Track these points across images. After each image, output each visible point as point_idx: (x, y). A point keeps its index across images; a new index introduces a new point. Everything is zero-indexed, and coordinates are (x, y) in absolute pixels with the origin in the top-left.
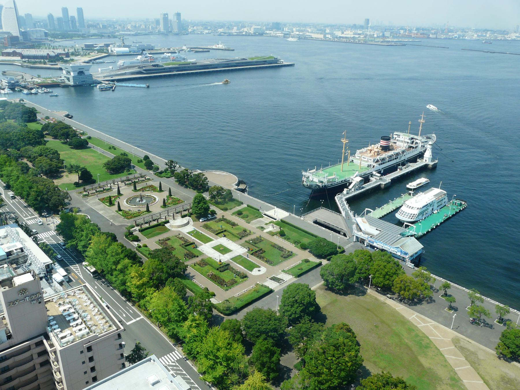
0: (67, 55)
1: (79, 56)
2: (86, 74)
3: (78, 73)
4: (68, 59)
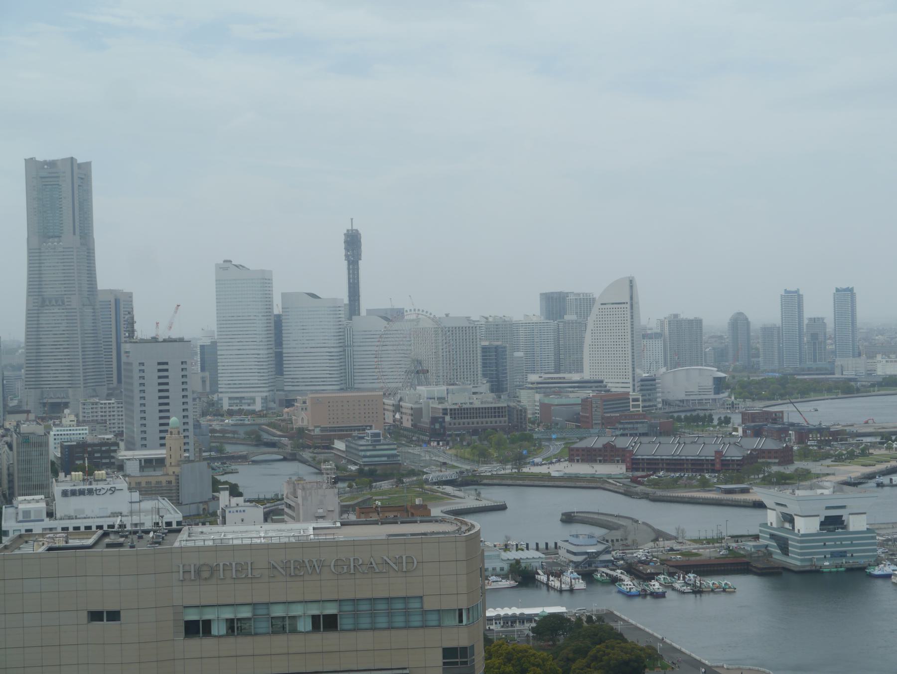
0: (786, 456)
1: (828, 462)
2: (851, 528)
3: (822, 524)
4: (789, 470)
